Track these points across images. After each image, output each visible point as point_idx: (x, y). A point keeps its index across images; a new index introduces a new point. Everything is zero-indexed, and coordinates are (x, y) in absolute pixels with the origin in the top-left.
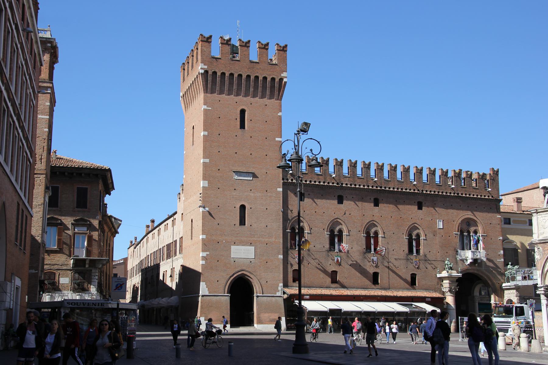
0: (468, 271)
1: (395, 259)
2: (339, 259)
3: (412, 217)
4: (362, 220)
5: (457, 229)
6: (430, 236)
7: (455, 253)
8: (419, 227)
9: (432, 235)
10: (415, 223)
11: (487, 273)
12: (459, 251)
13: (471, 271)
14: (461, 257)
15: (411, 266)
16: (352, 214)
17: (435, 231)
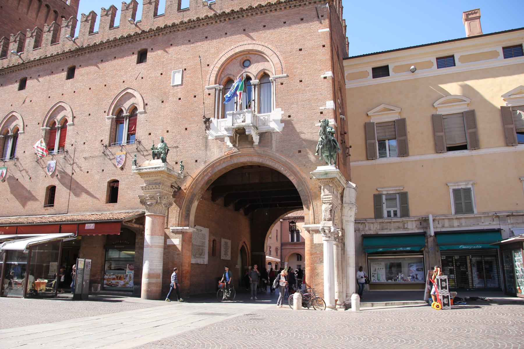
0: (235, 161)
1: (85, 158)
2: (5, 172)
3: (125, 79)
4: (46, 106)
5: (213, 79)
6: (154, 103)
7: (204, 126)
8: (135, 93)
9: (158, 103)
10: (128, 88)
11: (284, 159)
12: (214, 121)
13: (244, 160)
14: (217, 130)
15: (109, 166)
16: (34, 99)
17: (165, 93)
